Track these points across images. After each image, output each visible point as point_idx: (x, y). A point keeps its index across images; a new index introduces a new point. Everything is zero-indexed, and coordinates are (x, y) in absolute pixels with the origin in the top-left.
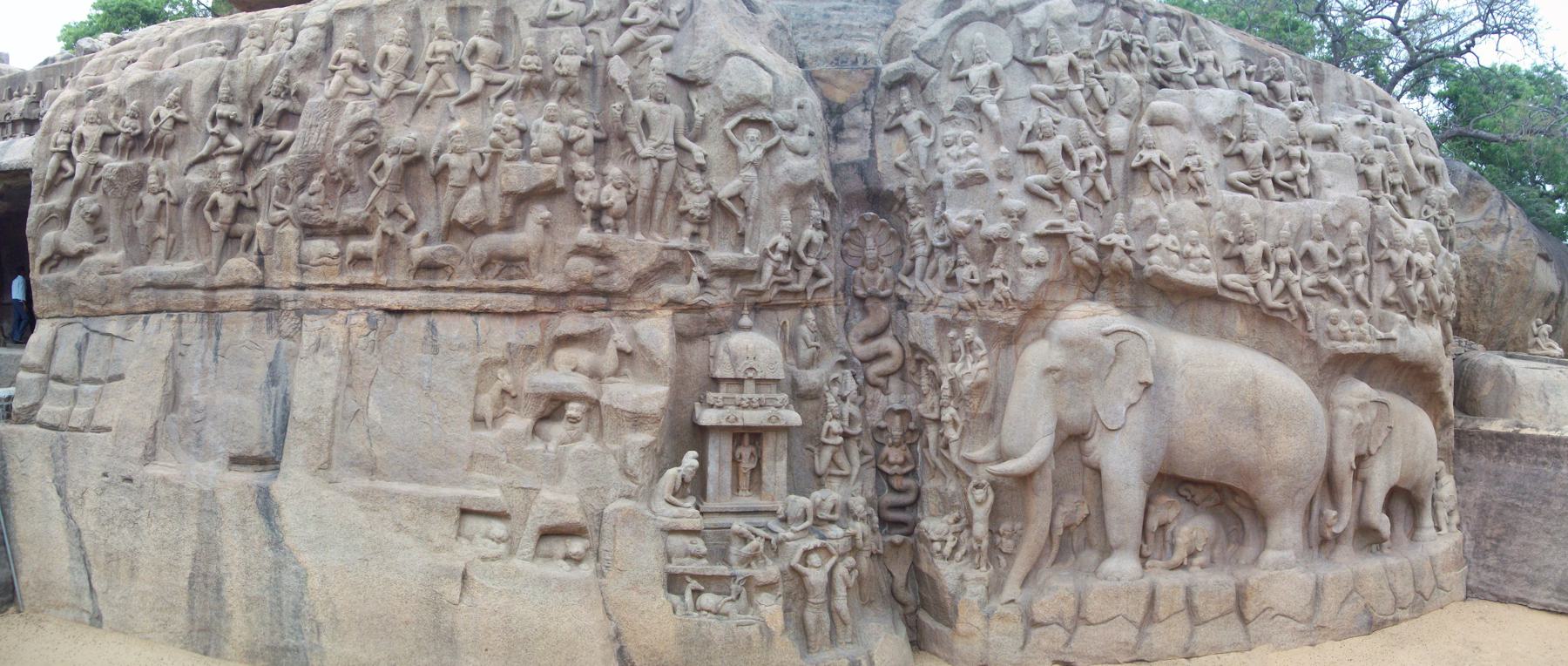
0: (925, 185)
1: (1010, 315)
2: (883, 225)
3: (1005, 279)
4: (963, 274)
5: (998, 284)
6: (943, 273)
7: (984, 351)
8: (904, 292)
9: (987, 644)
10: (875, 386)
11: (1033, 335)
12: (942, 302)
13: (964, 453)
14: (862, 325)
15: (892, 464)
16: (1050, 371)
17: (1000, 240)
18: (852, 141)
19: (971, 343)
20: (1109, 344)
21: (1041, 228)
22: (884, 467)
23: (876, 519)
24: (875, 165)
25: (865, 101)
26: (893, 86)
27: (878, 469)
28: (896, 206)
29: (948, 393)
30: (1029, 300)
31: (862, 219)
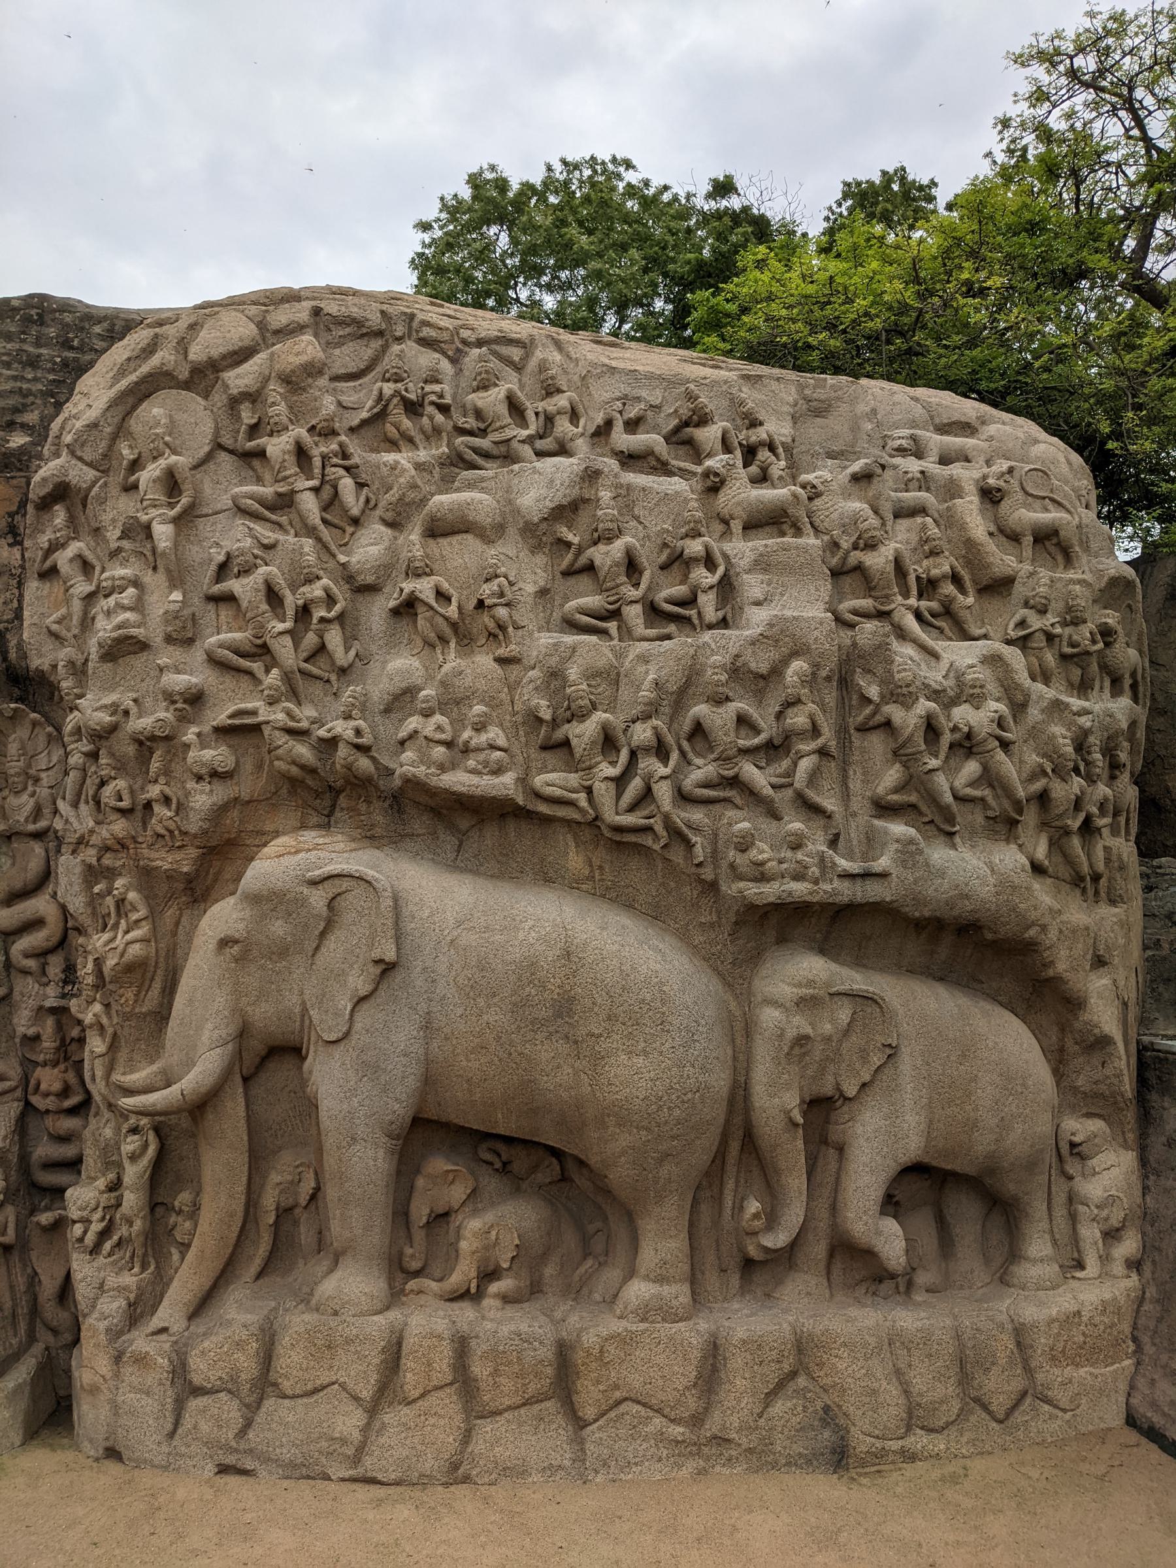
1: (178, 856)
2: (34, 724)
3: (167, 800)
4: (108, 791)
5: (160, 810)
6: (91, 793)
7: (142, 912)
8: (58, 824)
9: (115, 1408)
10: (26, 972)
11: (232, 887)
13: (117, 1077)
15: (46, 1095)
16: (225, 943)
17: (153, 738)
20: (318, 899)
21: (222, 717)
22: (35, 1100)
26: (45, 504)
27: (28, 1104)
29: (90, 980)
30: (205, 832)
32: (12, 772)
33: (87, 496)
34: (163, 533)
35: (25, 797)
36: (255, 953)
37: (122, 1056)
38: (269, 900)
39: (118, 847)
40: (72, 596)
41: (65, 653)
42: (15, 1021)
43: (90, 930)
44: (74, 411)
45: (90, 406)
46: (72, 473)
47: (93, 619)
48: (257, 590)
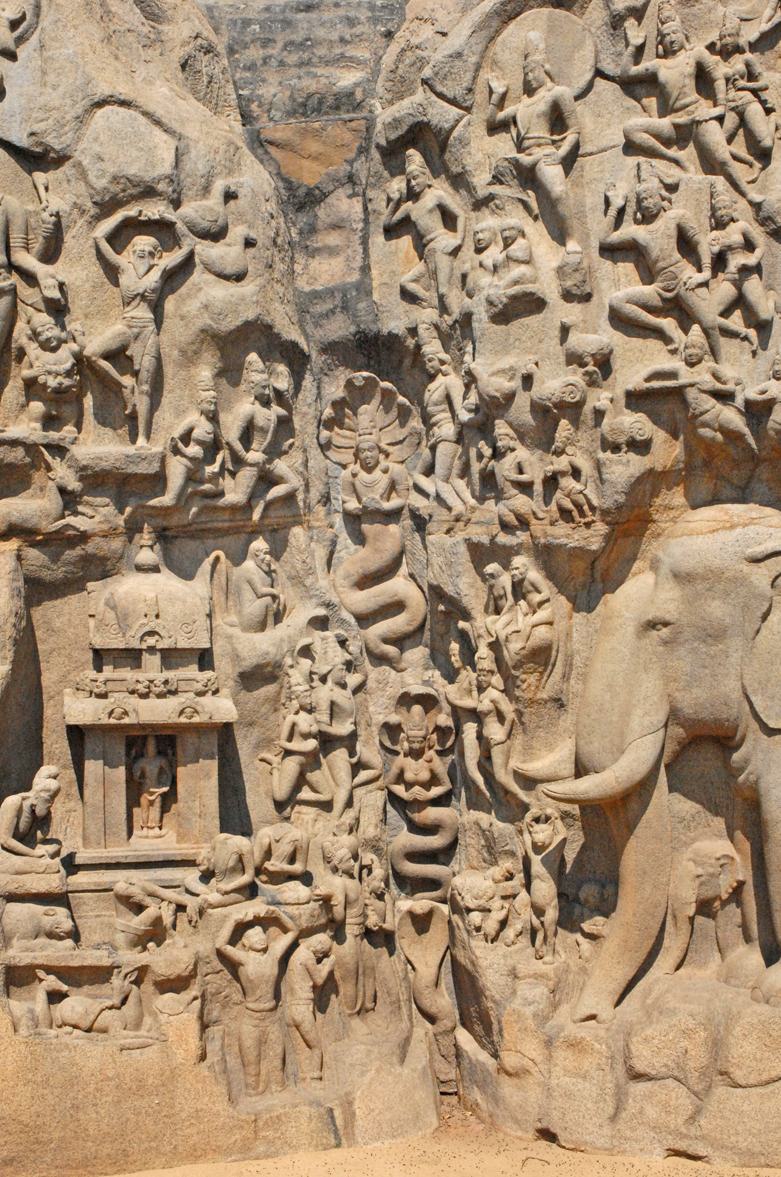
0: (449, 320)
1: (586, 533)
2: (386, 393)
3: (576, 473)
4: (505, 468)
5: (567, 483)
12: (475, 517)
13: (514, 763)
14: (354, 558)
16: (652, 625)
18: (332, 251)
19: (523, 580)
22: (399, 790)
23: (378, 872)
24: (369, 293)
25: (351, 179)
28: (407, 362)
30: (619, 508)
31: (349, 384)
32: (362, 446)
33: (448, 138)
34: (552, 174)
35: (377, 473)
36: (687, 634)
37: (518, 741)
38: (704, 578)
39: (517, 523)
40: (434, 251)
41: (427, 315)
42: (371, 709)
43: (474, 613)
44: (415, 41)
45: (444, 34)
46: (430, 110)
47: (464, 277)
48: (669, 236)
